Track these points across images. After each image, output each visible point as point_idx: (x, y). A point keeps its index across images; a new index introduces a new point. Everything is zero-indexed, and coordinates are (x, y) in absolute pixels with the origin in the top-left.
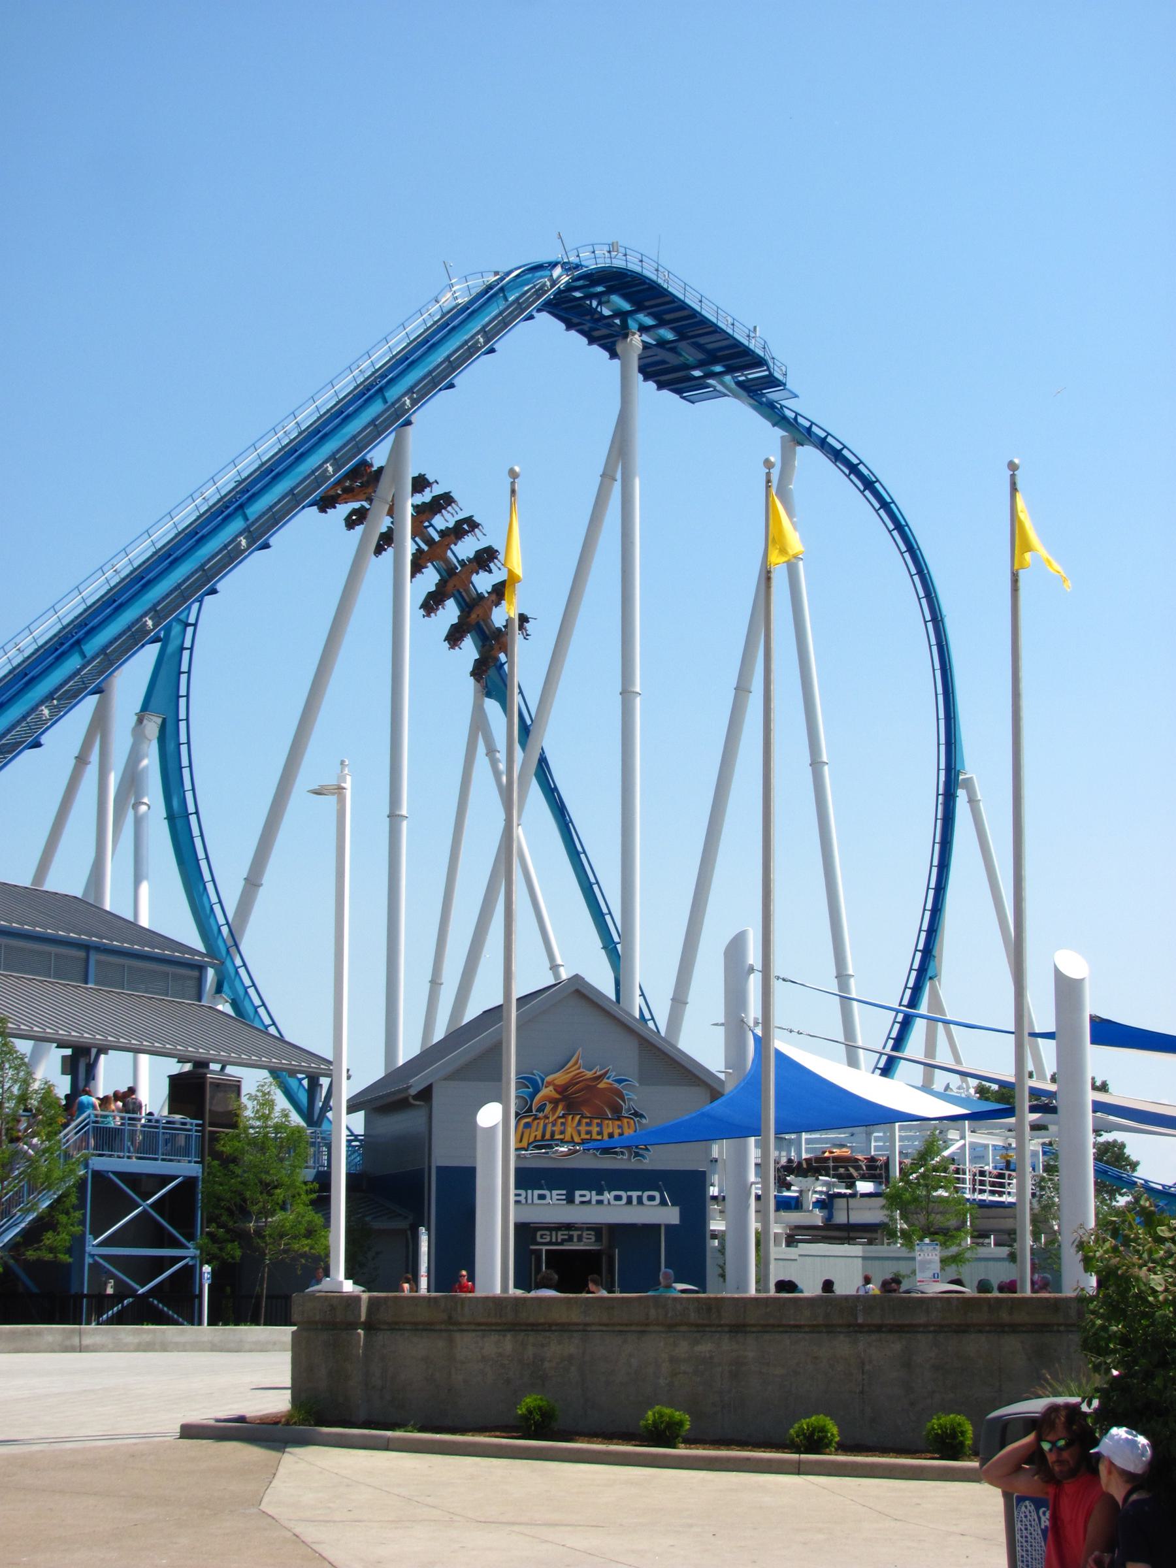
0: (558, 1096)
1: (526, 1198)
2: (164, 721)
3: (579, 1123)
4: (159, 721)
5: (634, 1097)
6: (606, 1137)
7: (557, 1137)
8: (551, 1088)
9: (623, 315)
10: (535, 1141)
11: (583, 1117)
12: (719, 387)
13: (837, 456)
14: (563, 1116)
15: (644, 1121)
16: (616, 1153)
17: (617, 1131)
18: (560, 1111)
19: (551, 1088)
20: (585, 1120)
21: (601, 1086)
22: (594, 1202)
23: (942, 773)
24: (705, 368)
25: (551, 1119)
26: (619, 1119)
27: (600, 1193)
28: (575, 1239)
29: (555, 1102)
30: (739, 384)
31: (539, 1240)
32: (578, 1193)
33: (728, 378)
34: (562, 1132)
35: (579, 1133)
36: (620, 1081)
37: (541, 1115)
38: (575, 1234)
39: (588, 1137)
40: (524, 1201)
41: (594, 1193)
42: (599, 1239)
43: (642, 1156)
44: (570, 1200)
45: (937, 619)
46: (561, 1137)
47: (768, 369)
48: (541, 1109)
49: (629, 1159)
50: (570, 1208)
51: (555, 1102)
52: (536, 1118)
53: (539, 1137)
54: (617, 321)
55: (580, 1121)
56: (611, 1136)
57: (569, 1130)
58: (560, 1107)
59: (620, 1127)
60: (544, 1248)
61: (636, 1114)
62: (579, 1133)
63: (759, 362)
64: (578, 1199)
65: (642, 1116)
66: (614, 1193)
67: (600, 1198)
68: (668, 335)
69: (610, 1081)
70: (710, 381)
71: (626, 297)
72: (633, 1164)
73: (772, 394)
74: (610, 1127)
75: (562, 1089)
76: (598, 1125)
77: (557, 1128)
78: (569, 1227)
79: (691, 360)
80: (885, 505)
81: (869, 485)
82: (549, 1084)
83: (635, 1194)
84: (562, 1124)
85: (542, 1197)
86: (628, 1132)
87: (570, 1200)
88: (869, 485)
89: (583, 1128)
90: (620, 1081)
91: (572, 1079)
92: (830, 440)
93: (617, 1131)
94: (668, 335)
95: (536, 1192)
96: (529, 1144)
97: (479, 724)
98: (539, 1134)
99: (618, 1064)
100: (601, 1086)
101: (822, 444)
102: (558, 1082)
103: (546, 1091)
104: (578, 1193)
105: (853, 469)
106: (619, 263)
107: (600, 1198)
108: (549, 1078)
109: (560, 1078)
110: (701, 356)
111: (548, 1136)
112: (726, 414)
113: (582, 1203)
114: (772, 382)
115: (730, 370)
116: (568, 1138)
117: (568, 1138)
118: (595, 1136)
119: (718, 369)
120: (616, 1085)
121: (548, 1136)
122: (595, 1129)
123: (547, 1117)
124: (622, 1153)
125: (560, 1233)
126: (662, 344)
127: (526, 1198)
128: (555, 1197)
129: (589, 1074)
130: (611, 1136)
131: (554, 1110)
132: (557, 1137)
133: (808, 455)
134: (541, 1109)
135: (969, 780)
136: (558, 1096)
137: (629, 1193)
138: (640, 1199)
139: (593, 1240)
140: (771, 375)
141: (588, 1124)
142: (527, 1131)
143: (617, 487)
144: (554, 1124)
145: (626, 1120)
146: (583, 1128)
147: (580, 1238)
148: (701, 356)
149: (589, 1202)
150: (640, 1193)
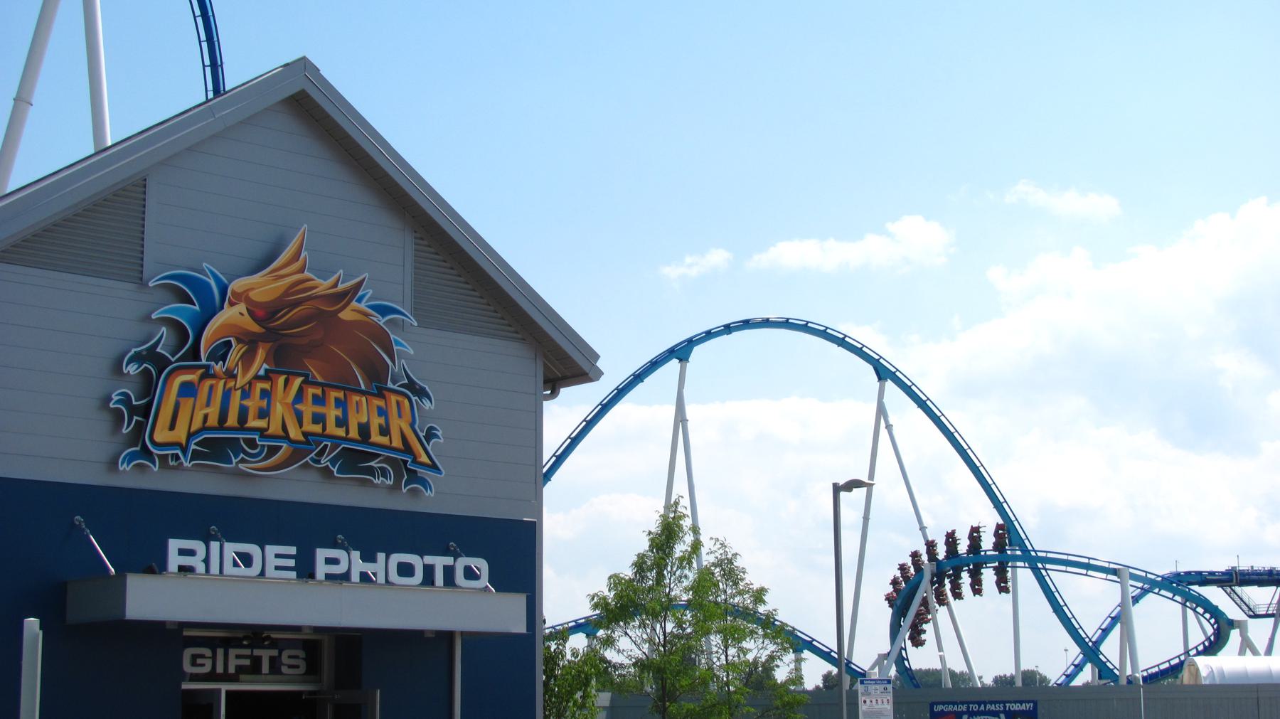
0: (255, 328)
1: (207, 561)
3: (300, 396)
5: (411, 351)
6: (354, 433)
7: (253, 423)
8: (242, 307)
10: (204, 429)
11: (308, 382)
14: (267, 377)
15: (427, 404)
16: (371, 471)
17: (376, 422)
18: (260, 365)
19: (242, 307)
20: (311, 391)
21: (346, 315)
22: (355, 577)
25: (241, 381)
26: (381, 393)
27: (368, 557)
28: (265, 668)
29: (251, 342)
31: (188, 668)
32: (322, 554)
34: (263, 414)
35: (299, 417)
36: (384, 311)
37: (218, 367)
38: (265, 654)
39: (317, 428)
40: (201, 568)
41: (356, 555)
42: (313, 668)
43: (424, 483)
44: (305, 570)
48: (221, 352)
49: (396, 487)
50: (308, 587)
51: (251, 342)
52: (207, 374)
53: (213, 421)
55: (301, 390)
56: (364, 430)
57: (279, 410)
58: (261, 354)
59: (382, 412)
60: (224, 687)
61: (411, 385)
62: (299, 417)
64: (322, 569)
65: (422, 393)
66: (396, 558)
67: (369, 568)
69: (362, 306)
72: (401, 502)
74: (363, 411)
75: (265, 313)
76: (339, 403)
77: (253, 404)
78: (255, 635)
82: (239, 297)
83: (440, 562)
84: (265, 394)
85: (246, 559)
86: (397, 424)
87: (305, 570)
90: (384, 311)
91: (287, 293)
93: (376, 422)
95: (231, 549)
96: (190, 436)
98: (214, 412)
99: (376, 270)
100: (346, 315)
102: (256, 296)
103: (231, 315)
104: (322, 554)
107: (369, 568)
108: (237, 285)
109: (262, 287)
111: (232, 420)
113: (329, 577)
116: (275, 428)
117: (275, 428)
118: (332, 429)
120: (381, 321)
121: (232, 420)
122: (332, 413)
123: (231, 375)
124: (384, 473)
125: (233, 652)
127: (207, 561)
128: (272, 562)
129: (323, 286)
130: (364, 430)
131: (248, 359)
132: (253, 423)
134: (221, 352)
136: (255, 328)
137: (429, 559)
138: (449, 572)
139: (302, 670)
141: (318, 400)
142: (187, 403)
144: (246, 394)
145: (393, 399)
146: (308, 409)
147: (275, 665)
149: (346, 577)
150: (449, 560)
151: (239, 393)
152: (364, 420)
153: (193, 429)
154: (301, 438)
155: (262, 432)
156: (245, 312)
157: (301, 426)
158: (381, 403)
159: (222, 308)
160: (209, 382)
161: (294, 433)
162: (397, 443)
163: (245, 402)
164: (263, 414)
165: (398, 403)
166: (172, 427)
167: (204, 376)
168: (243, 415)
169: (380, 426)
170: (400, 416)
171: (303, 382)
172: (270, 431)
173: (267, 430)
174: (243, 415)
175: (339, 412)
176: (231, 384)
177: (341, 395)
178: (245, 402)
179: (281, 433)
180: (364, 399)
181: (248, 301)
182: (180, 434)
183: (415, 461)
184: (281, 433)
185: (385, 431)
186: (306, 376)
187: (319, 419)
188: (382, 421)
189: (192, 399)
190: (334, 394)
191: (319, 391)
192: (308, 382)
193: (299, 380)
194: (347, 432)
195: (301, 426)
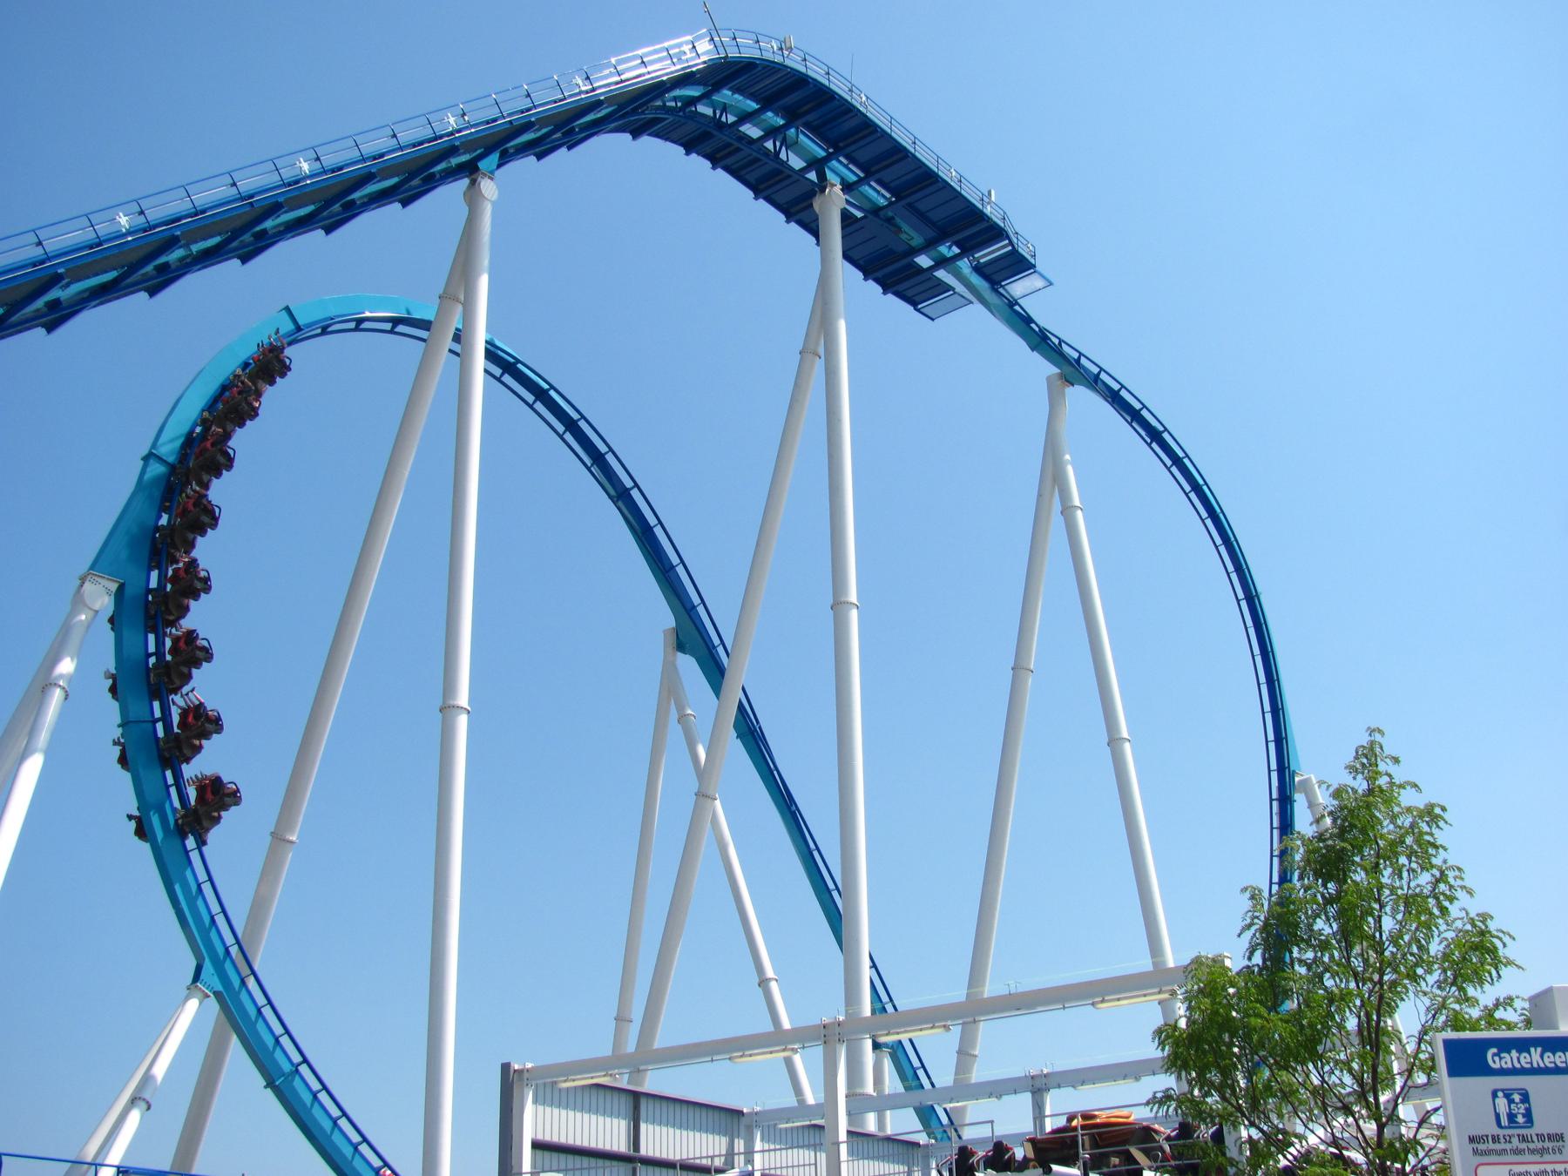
2: (121, 588)
4: (114, 587)
9: (818, 164)
12: (960, 288)
13: (1115, 398)
23: (1274, 775)
24: (933, 253)
30: (978, 269)
33: (964, 265)
45: (1251, 599)
47: (1011, 243)
54: (812, 176)
63: (996, 233)
68: (877, 195)
70: (941, 274)
71: (817, 131)
73: (1018, 288)
79: (917, 240)
80: (1177, 461)
81: (1155, 436)
88: (1155, 436)
92: (1103, 376)
94: (877, 195)
97: (670, 689)
101: (1094, 381)
105: (1134, 415)
106: (794, 62)
110: (931, 233)
112: (969, 327)
114: (1018, 264)
115: (967, 249)
119: (948, 250)
126: (875, 211)
133: (1080, 398)
135: (1306, 782)
140: (1014, 252)
143: (819, 365)
148: (931, 233)
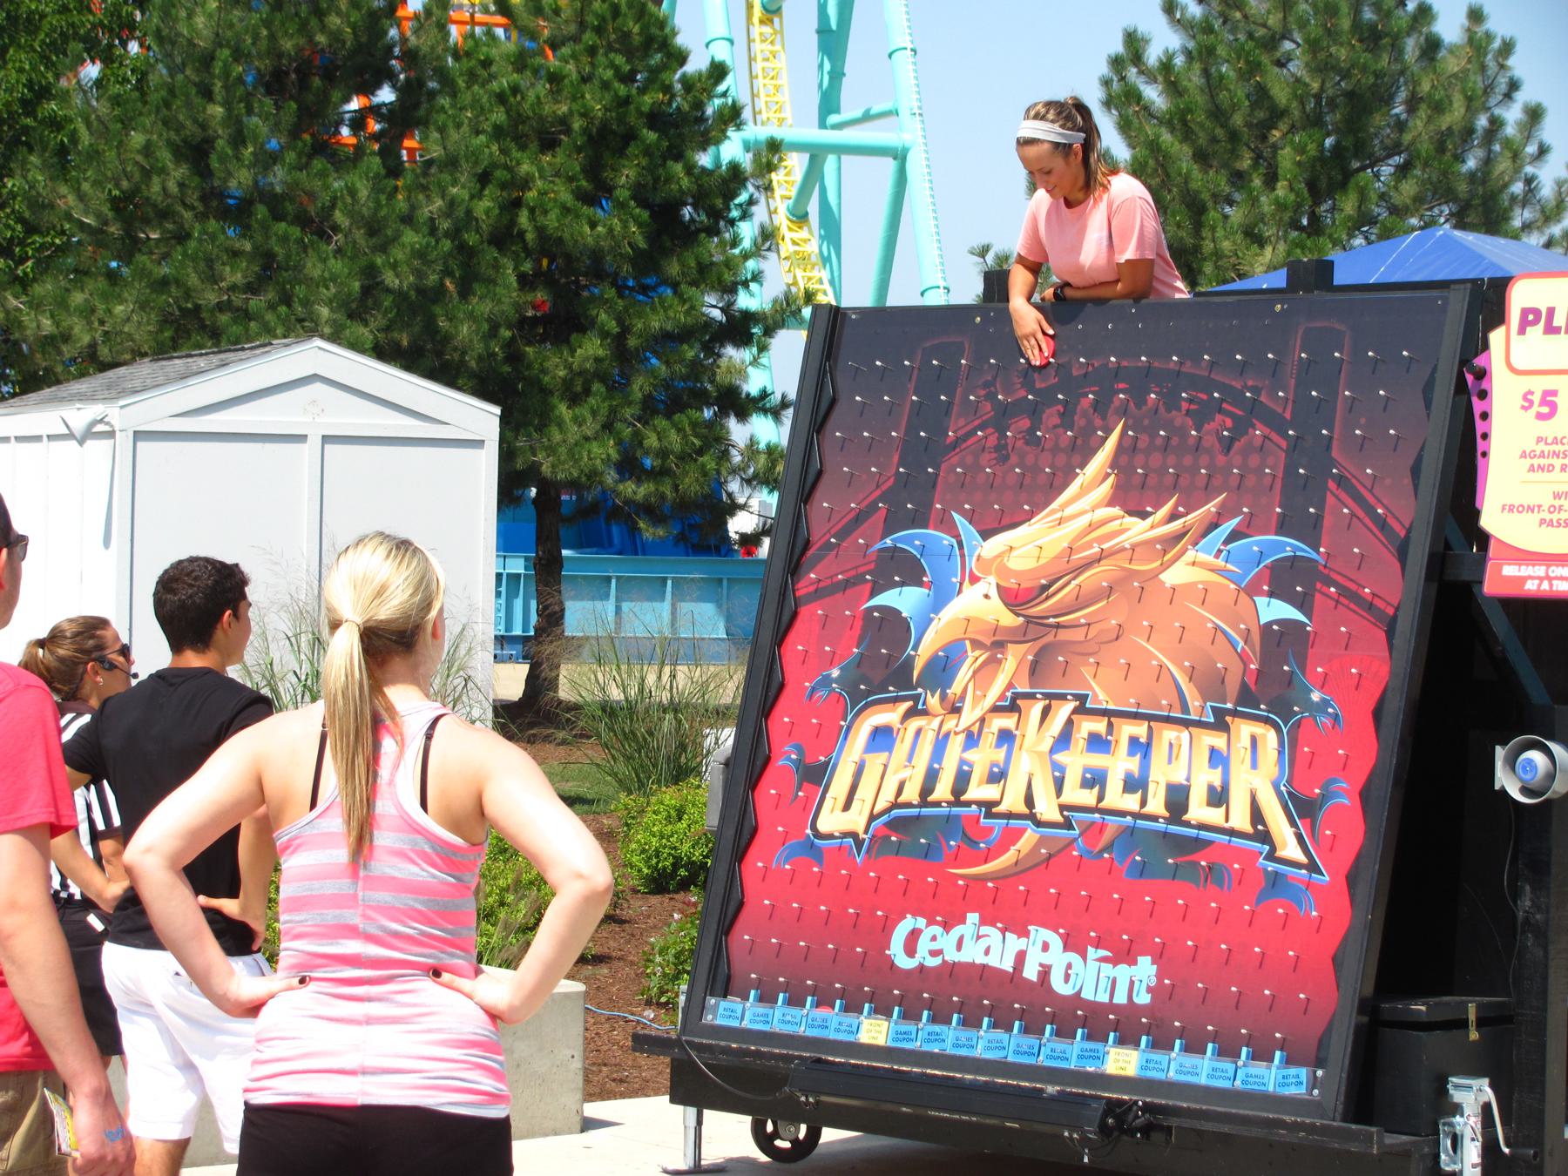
0: (1008, 619)
3: (1064, 739)
6: (1157, 805)
11: (1083, 708)
20: (1088, 726)
25: (969, 716)
39: (1088, 797)
46: (990, 792)
51: (997, 643)
53: (911, 794)
56: (1177, 800)
77: (984, 756)
84: (1006, 737)
89: (1076, 760)
93: (1203, 778)
111: (942, 791)
117: (1013, 801)
118: (1116, 798)
121: (942, 791)
130: (1177, 800)
132: (977, 791)
136: (1008, 619)
142: (875, 762)
151: (962, 737)
152: (1179, 777)
153: (876, 811)
154: (1057, 817)
155: (989, 806)
156: (994, 593)
157: (1059, 792)
158: (1219, 741)
159: (960, 591)
160: (915, 723)
161: (1047, 808)
162: (1240, 819)
163: (969, 756)
164: (997, 776)
165: (1254, 740)
166: (847, 806)
167: (909, 714)
168: (962, 780)
169: (1211, 788)
170: (1254, 765)
171: (1075, 711)
172: (1002, 808)
173: (997, 803)
174: (962, 780)
175: (1133, 765)
176: (950, 724)
177: (1141, 730)
178: (969, 756)
179: (1024, 810)
180: (1185, 735)
181: (1003, 571)
182: (856, 820)
183: (1271, 856)
184: (1024, 810)
185: (1218, 797)
186: (1082, 699)
187: (1095, 780)
188: (1216, 778)
189: (885, 755)
190: (1128, 729)
191: (1100, 726)
192: (1082, 710)
193: (1064, 710)
194: (1143, 803)
195: (1059, 792)
